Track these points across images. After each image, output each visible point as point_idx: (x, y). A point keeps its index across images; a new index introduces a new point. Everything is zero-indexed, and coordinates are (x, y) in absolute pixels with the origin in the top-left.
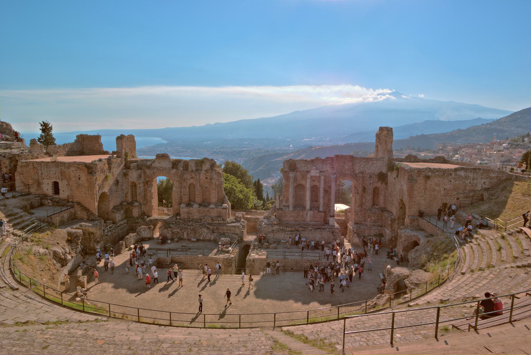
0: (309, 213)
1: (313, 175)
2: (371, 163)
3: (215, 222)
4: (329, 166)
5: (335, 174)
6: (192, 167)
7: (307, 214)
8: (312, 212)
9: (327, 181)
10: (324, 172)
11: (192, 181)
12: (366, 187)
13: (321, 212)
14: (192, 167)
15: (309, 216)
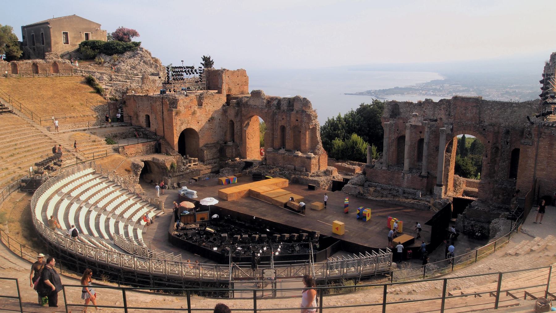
0: (406, 177)
1: (413, 124)
2: (509, 111)
3: (297, 172)
4: (443, 112)
5: (452, 124)
6: (284, 107)
7: (403, 177)
8: (410, 175)
9: (436, 134)
10: (436, 120)
11: (282, 123)
12: (500, 148)
13: (423, 177)
14: (284, 107)
15: (406, 180)
